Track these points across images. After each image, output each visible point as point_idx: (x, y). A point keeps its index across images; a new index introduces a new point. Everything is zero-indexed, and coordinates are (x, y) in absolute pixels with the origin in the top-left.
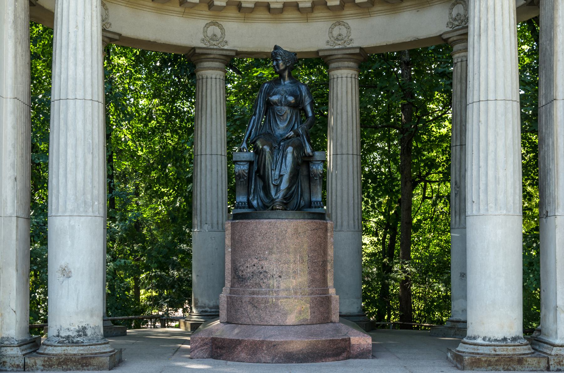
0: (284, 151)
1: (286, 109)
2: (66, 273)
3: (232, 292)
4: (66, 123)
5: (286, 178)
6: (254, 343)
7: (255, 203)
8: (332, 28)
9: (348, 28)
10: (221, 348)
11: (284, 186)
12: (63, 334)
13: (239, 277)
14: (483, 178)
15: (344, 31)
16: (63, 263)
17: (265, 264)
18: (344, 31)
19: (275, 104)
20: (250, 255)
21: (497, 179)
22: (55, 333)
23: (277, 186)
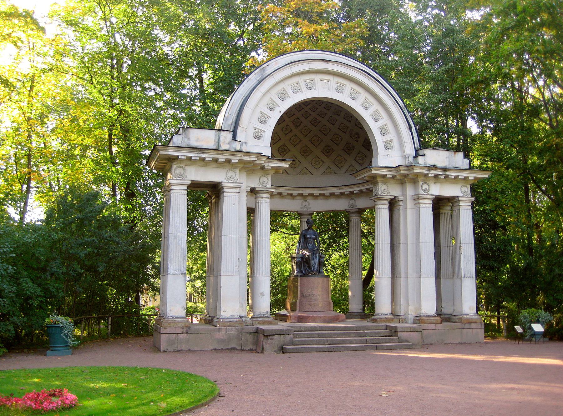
0: (316, 255)
1: (311, 240)
2: (262, 294)
3: (300, 301)
4: (263, 247)
5: (317, 264)
6: (314, 317)
7: (303, 272)
8: (302, 203)
9: (309, 203)
10: (302, 319)
11: (316, 266)
12: (262, 314)
13: (304, 296)
14: (381, 266)
15: (307, 204)
16: (262, 291)
17: (314, 292)
18: (307, 204)
19: (309, 238)
20: (308, 289)
21: (385, 266)
22: (259, 314)
23: (314, 266)
